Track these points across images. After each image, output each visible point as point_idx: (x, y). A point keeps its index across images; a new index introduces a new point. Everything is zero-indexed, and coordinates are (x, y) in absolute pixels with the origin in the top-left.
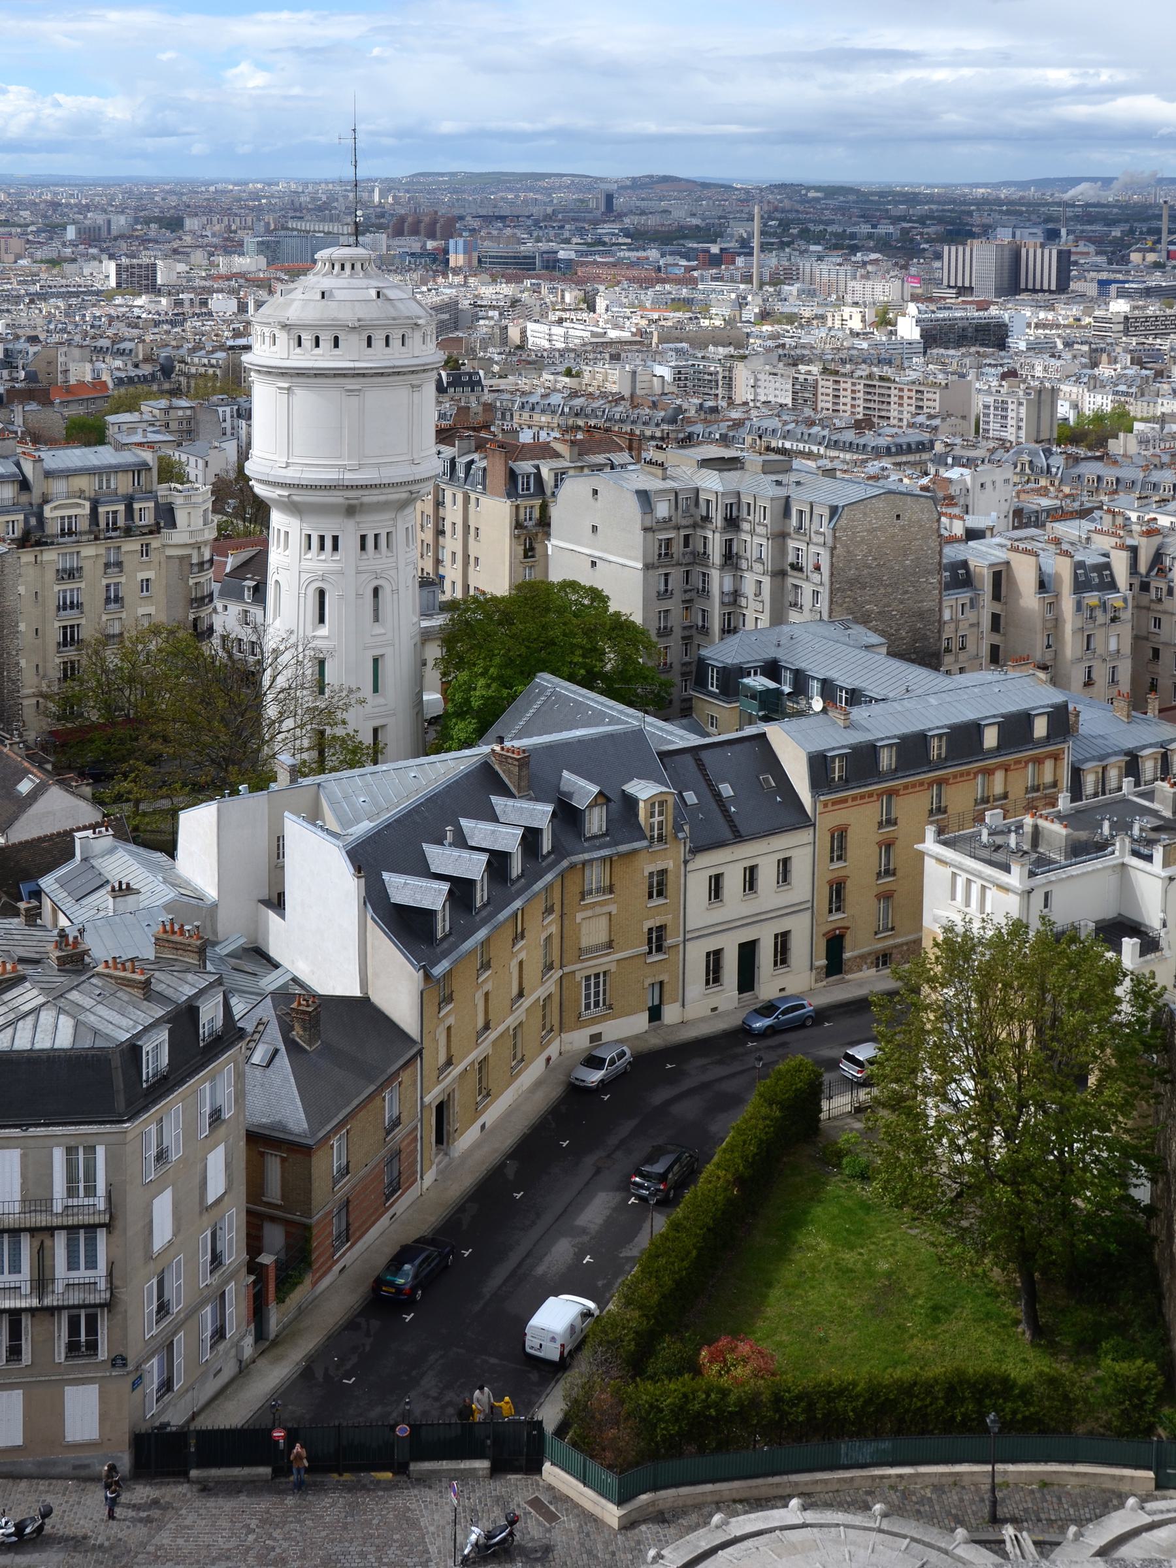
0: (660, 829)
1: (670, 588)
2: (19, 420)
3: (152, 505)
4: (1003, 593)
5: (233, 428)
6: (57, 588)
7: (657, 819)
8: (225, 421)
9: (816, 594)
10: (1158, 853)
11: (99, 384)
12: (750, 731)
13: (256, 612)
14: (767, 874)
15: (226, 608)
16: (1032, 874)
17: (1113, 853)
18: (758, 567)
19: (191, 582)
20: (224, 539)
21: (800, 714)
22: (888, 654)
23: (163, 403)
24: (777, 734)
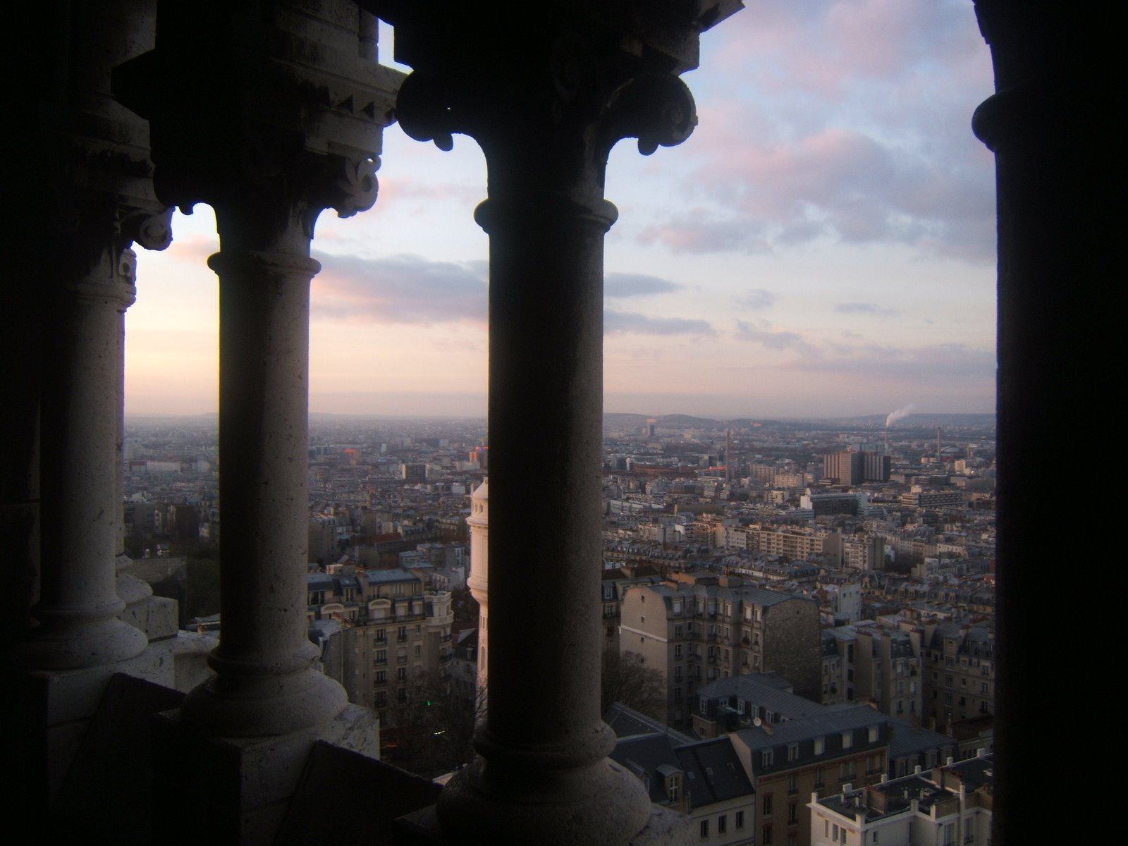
0: (676, 793)
1: (681, 654)
2: (357, 554)
3: (421, 603)
4: (854, 658)
5: (462, 560)
6: (374, 650)
7: (674, 788)
8: (458, 556)
9: (756, 657)
10: (933, 809)
11: (396, 534)
12: (722, 737)
13: (472, 664)
14: (731, 822)
15: (458, 663)
16: (867, 822)
17: (910, 810)
18: (726, 642)
19: (441, 648)
20: (456, 627)
21: (748, 727)
22: (794, 693)
23: (428, 545)
24: (735, 738)
